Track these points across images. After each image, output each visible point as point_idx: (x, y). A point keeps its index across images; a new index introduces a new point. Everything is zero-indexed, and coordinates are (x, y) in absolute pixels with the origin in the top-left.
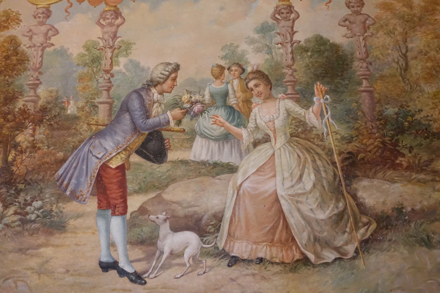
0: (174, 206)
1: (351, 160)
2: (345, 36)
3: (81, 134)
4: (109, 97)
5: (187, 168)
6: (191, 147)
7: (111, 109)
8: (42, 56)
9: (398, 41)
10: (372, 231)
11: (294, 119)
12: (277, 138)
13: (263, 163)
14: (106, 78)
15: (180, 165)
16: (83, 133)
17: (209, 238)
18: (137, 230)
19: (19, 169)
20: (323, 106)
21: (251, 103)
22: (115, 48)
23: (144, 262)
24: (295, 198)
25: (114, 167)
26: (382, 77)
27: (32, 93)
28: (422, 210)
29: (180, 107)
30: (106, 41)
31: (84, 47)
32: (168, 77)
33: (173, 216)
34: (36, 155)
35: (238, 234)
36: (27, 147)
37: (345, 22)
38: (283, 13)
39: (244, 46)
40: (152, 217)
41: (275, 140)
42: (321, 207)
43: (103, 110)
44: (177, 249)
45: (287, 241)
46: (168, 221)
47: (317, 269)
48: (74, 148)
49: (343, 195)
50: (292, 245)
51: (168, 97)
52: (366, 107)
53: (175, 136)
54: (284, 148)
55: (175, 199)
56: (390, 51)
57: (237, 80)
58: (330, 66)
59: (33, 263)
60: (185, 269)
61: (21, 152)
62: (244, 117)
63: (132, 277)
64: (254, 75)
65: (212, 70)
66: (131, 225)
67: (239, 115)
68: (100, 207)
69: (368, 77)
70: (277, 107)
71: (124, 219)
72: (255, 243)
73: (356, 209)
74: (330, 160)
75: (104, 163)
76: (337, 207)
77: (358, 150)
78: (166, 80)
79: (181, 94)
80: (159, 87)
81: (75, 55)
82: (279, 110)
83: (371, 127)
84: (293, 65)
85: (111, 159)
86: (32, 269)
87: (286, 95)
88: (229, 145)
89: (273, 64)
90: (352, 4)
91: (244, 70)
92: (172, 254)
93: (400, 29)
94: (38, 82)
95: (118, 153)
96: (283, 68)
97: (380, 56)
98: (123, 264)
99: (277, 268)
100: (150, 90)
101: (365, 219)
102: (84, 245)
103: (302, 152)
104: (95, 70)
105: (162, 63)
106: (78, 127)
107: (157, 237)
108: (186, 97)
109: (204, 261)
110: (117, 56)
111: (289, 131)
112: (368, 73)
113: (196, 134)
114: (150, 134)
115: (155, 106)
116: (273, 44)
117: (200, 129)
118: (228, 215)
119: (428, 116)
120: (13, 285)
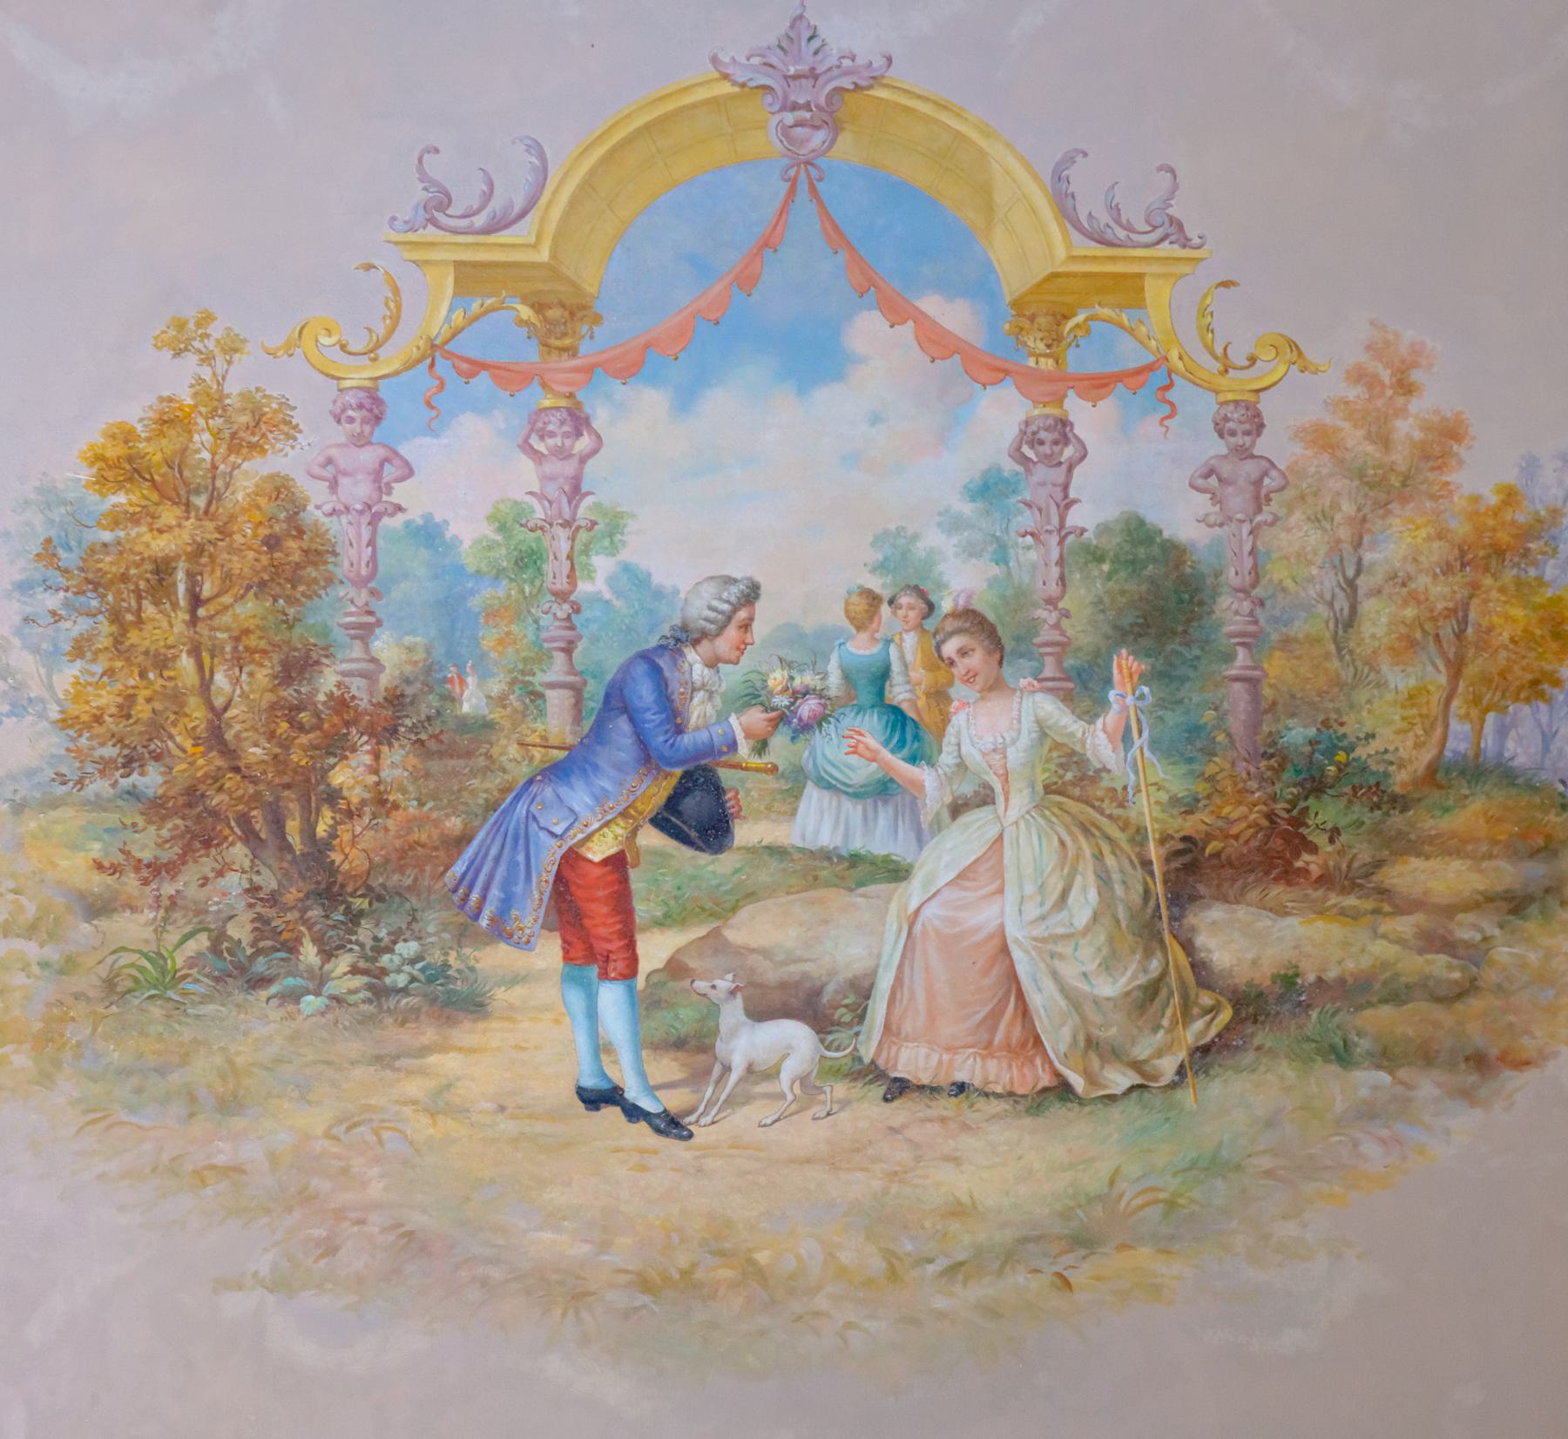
0: (755, 960)
1: (1187, 858)
3: (504, 771)
4: (572, 671)
5: (783, 865)
6: (793, 812)
7: (578, 705)
8: (372, 543)
9: (1339, 541)
10: (1221, 1026)
11: (1057, 746)
13: (973, 858)
14: (560, 614)
15: (766, 858)
16: (509, 766)
17: (842, 1036)
18: (664, 1016)
19: (349, 858)
20: (1132, 713)
21: (949, 700)
22: (579, 528)
23: (686, 1090)
25: (597, 858)
26: (1287, 643)
27: (357, 651)
28: (1341, 981)
29: (762, 704)
30: (550, 502)
31: (492, 518)
32: (729, 618)
33: (752, 984)
34: (390, 823)
35: (907, 1027)
36: (363, 802)
38: (1042, 443)
39: (933, 539)
40: (701, 985)
41: (1007, 800)
42: (1107, 968)
43: (558, 701)
44: (764, 1059)
45: (1023, 1045)
46: (739, 996)
47: (1087, 1109)
49: (1162, 941)
50: (1034, 1056)
51: (732, 677)
52: (1237, 724)
53: (752, 780)
54: (1027, 821)
55: (753, 945)
56: (1314, 571)
57: (912, 634)
59: (415, 1088)
61: (349, 814)
62: (928, 737)
63: (658, 1121)
64: (957, 624)
65: (847, 603)
66: (646, 1005)
68: (567, 958)
69: (1252, 640)
70: (1015, 713)
71: (631, 990)
72: (948, 1049)
74: (1139, 855)
75: (570, 849)
76: (1145, 971)
77: (1207, 834)
78: (722, 628)
79: (764, 668)
80: (705, 646)
81: (467, 544)
82: (1019, 721)
83: (1244, 775)
86: (415, 1103)
87: (1040, 681)
88: (890, 809)
89: (1010, 592)
90: (1231, 425)
91: (931, 607)
92: (753, 1073)
93: (1348, 508)
94: (371, 619)
95: (607, 824)
96: (1035, 605)
97: (1288, 583)
98: (633, 1094)
99: (997, 1106)
100: (682, 654)
101: (1206, 999)
102: (536, 1048)
103: (1071, 833)
104: (527, 589)
105: (712, 578)
106: (495, 751)
108: (777, 678)
109: (828, 1089)
110: (586, 551)
111: (1041, 777)
112: (1252, 628)
113: (806, 778)
114: (687, 775)
115: (696, 701)
116: (1013, 534)
117: (815, 764)
119: (1386, 751)
120: (372, 1139)
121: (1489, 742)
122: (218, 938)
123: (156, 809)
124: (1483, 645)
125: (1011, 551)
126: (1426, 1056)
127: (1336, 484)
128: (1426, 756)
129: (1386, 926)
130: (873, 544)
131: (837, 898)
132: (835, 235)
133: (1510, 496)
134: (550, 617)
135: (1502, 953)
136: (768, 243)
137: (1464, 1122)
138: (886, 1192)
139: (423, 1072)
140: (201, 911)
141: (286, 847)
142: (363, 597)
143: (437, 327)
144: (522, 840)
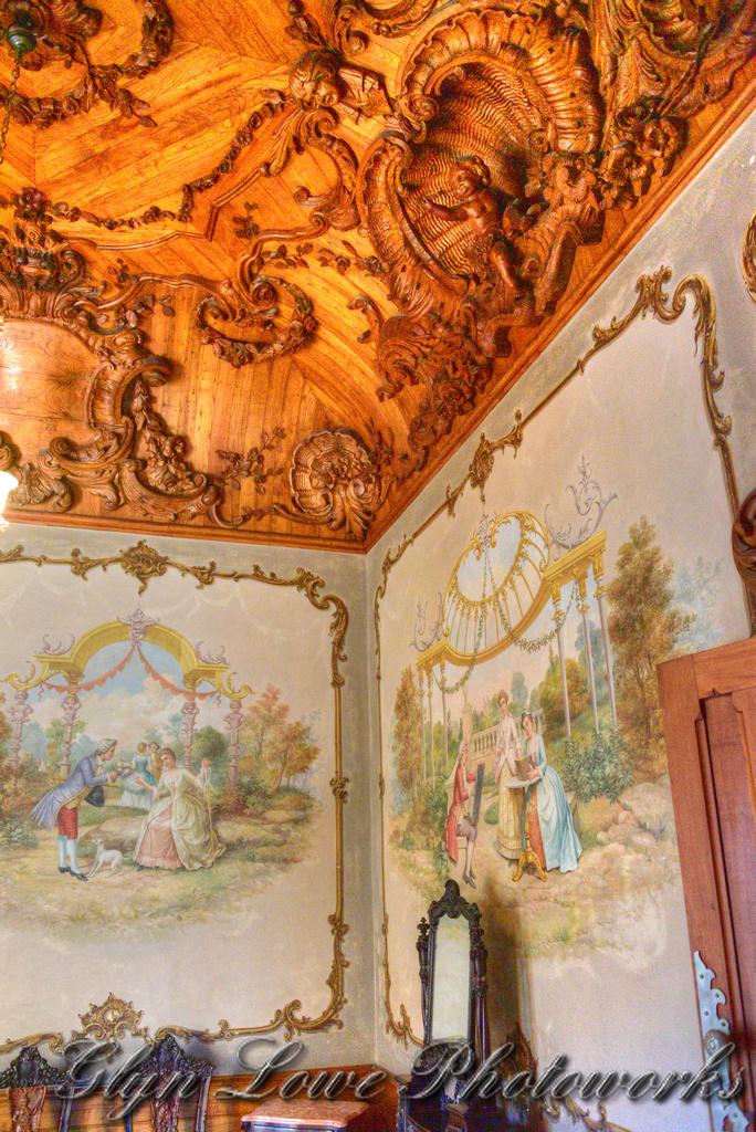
17: (128, 854)
24: (182, 832)
26: (244, 758)
27: (14, 755)
28: (254, 841)
37: (228, 718)
39: (161, 731)
43: (63, 769)
44: (108, 860)
48: (44, 795)
51: (108, 763)
58: (215, 748)
59: (17, 867)
61: (8, 796)
66: (80, 846)
67: (153, 777)
68: (60, 833)
69: (236, 757)
92: (104, 864)
93: (260, 726)
98: (74, 869)
99: (164, 873)
101: (220, 845)
107: (96, 853)
108: (119, 764)
118: (140, 840)
124: (290, 759)
126: (273, 860)
128: (276, 785)
129: (265, 827)
132: (142, 658)
133: (298, 724)
135: (292, 834)
136: (127, 660)
137: (281, 876)
139: (20, 863)
142: (17, 741)
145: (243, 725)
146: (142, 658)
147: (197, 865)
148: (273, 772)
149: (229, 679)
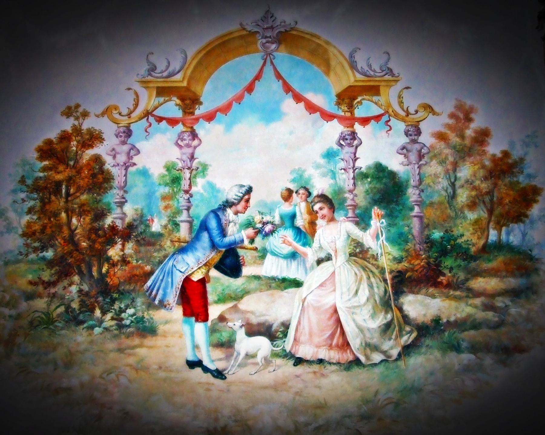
0: (249, 315)
2: (402, 164)
3: (165, 250)
4: (189, 216)
6: (263, 264)
8: (125, 175)
9: (448, 170)
11: (353, 240)
12: (338, 257)
15: (253, 279)
16: (167, 249)
17: (279, 342)
22: (193, 169)
24: (352, 310)
26: (432, 204)
27: (118, 210)
29: (252, 227)
30: (184, 161)
32: (242, 199)
35: (303, 338)
36: (118, 261)
37: (404, 150)
38: (347, 139)
41: (336, 259)
44: (251, 351)
45: (343, 346)
46: (243, 327)
47: (366, 369)
48: (160, 262)
51: (242, 218)
52: (416, 230)
58: (387, 190)
60: (258, 367)
66: (213, 330)
67: (306, 235)
68: (186, 314)
69: (420, 203)
70: (339, 229)
73: (401, 319)
75: (187, 277)
76: (386, 318)
77: (406, 270)
79: (253, 215)
80: (234, 208)
84: (354, 190)
85: (193, 273)
87: (347, 218)
89: (337, 188)
90: (410, 133)
91: (310, 194)
92: (248, 356)
93: (451, 159)
94: (124, 200)
95: (199, 268)
96: (345, 193)
97: (431, 184)
99: (334, 368)
100: (226, 210)
101: (408, 329)
103: (359, 270)
104: (175, 190)
106: (162, 243)
110: (195, 177)
111: (348, 251)
112: (420, 199)
113: (267, 252)
114: (226, 251)
115: (230, 226)
119: (468, 241)
121: (504, 237)
122: (68, 307)
123: (50, 263)
125: (337, 175)
127: (447, 151)
128: (482, 242)
129: (471, 301)
130: (291, 173)
131: (278, 293)
132: (279, 76)
134: (182, 199)
135: (513, 311)
136: (258, 77)
138: (294, 399)
140: (62, 298)
141: (92, 276)
142: (121, 193)
143: (150, 108)
144: (171, 273)
145: (426, 159)
146: (279, 76)
147: (377, 357)
148: (477, 222)
149: (400, 97)
